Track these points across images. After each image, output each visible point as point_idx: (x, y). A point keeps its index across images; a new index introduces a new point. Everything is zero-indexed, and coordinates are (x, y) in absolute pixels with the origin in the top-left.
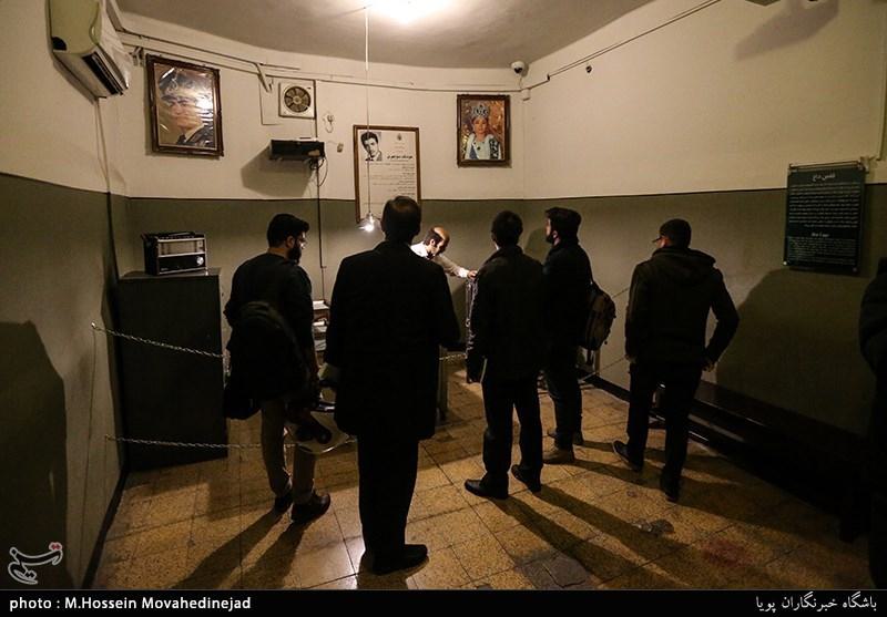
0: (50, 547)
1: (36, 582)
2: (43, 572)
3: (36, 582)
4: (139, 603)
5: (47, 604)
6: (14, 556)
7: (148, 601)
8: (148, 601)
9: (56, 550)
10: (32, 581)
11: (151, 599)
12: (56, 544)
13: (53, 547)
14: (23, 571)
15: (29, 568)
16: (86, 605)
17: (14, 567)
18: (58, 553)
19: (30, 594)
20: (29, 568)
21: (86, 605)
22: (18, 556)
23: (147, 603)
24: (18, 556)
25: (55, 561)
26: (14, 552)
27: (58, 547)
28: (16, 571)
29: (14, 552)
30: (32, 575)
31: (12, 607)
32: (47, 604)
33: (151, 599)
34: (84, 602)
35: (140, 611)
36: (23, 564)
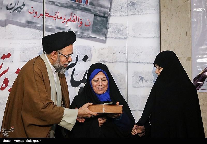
0: (11, 128)
1: (8, 136)
2: (10, 134)
3: (8, 136)
4: (25, 141)
5: (10, 141)
6: (3, 130)
7: (27, 140)
8: (27, 140)
9: (13, 128)
10: (7, 136)
11: (28, 140)
12: (13, 127)
13: (12, 128)
14: (5, 133)
15: (7, 133)
16: (15, 141)
17: (3, 132)
18: (13, 129)
19: (6, 138)
20: (7, 133)
21: (15, 141)
22: (4, 130)
23: (27, 141)
24: (4, 130)
25: (13, 131)
26: (3, 129)
27: (13, 128)
28: (3, 133)
29: (3, 129)
30: (7, 134)
31: (3, 142)
32: (10, 141)
33: (28, 140)
34: (14, 141)
35: (25, 142)
36: (5, 132)
